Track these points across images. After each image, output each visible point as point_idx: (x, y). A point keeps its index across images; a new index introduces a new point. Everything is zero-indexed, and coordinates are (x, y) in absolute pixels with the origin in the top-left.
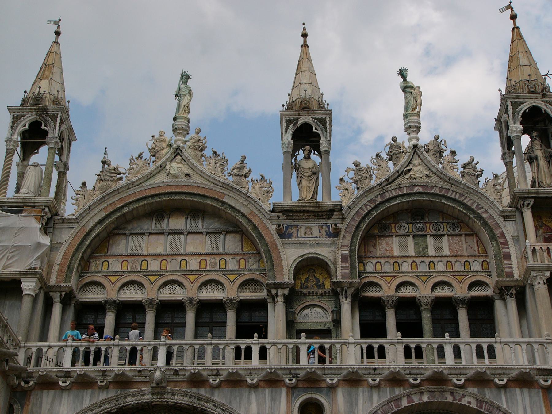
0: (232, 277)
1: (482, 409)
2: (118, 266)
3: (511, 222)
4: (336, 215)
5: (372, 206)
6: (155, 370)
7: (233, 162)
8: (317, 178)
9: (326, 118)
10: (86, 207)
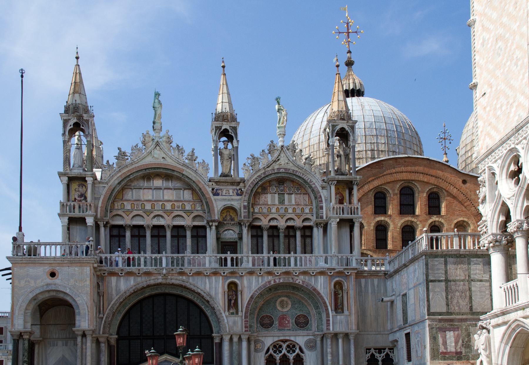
0: (189, 214)
5: (260, 179)
6: (163, 269)
7: (188, 152)
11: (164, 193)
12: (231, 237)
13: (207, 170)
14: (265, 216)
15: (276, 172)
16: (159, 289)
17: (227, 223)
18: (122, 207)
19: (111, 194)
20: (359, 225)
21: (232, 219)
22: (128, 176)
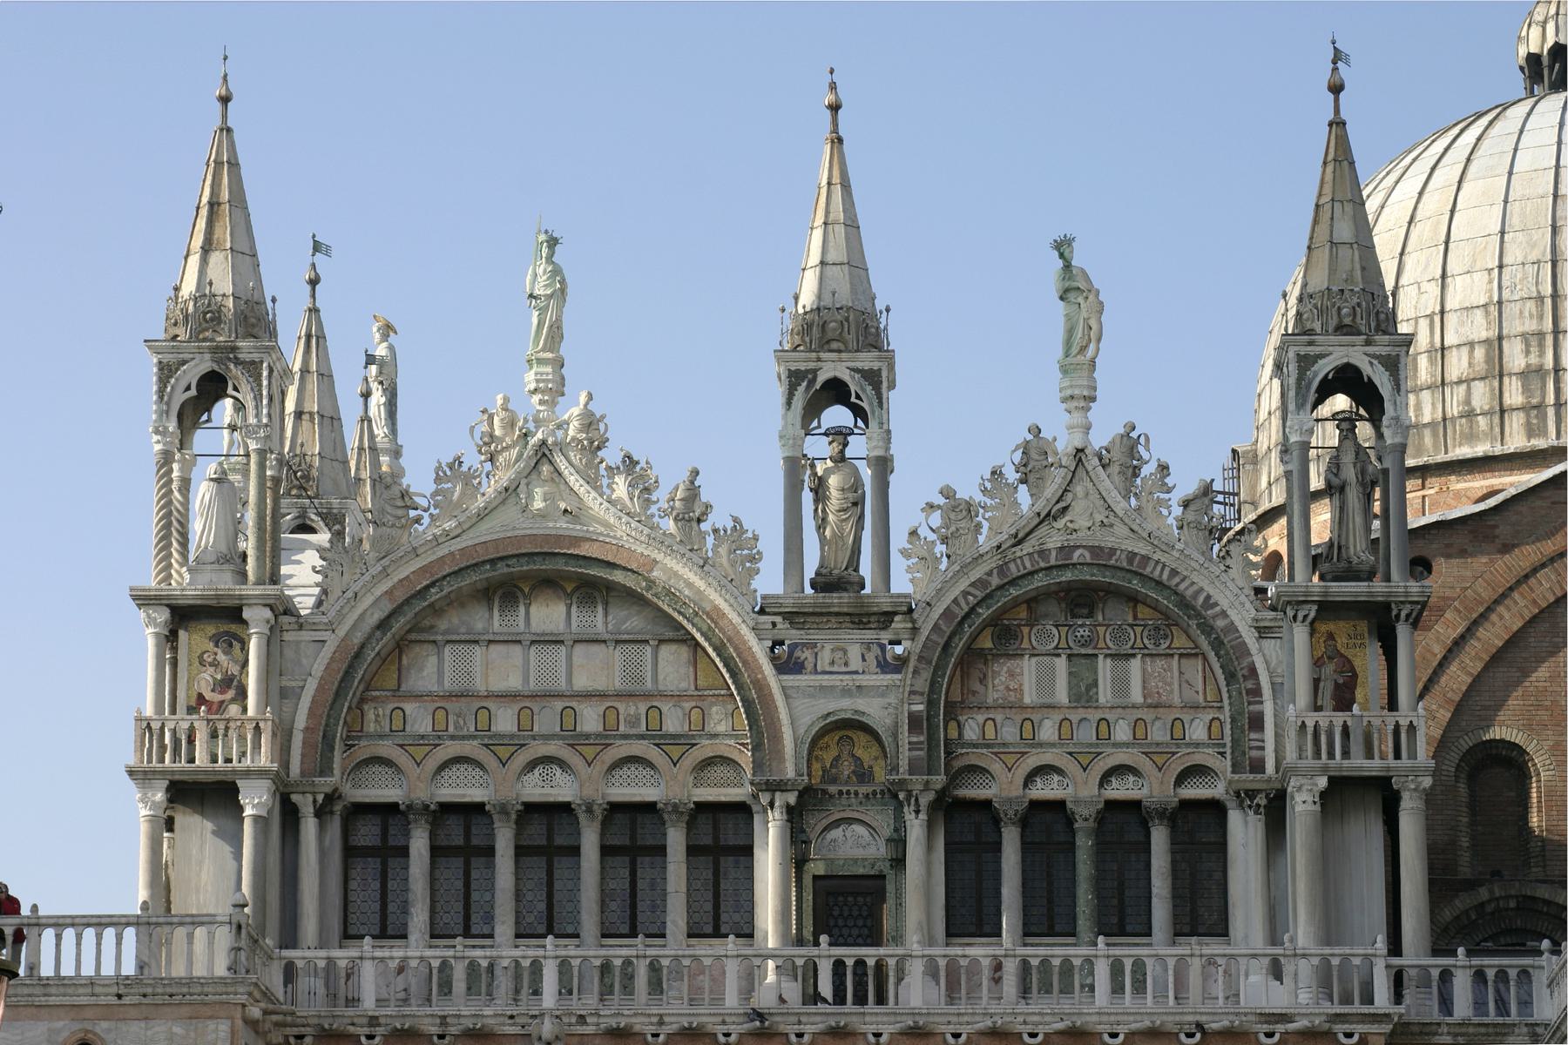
0: (676, 752)
2: (425, 722)
3: (1273, 641)
4: (900, 622)
5: (980, 594)
7: (669, 481)
8: (861, 517)
9: (880, 370)
11: (574, 658)
12: (859, 853)
13: (753, 559)
15: (1053, 562)
17: (841, 793)
18: (397, 725)
20: (1420, 804)
22: (420, 592)
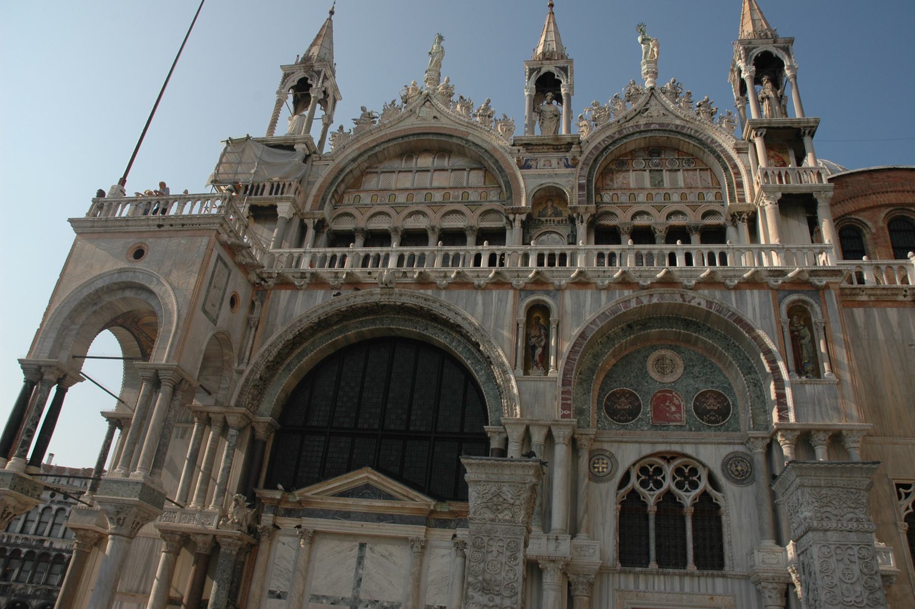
1: (711, 309)
4: (575, 148)
5: (610, 141)
7: (478, 105)
9: (567, 67)
10: (341, 146)
14: (625, 208)
16: (378, 322)
17: (547, 220)
19: (336, 177)
21: (558, 214)
